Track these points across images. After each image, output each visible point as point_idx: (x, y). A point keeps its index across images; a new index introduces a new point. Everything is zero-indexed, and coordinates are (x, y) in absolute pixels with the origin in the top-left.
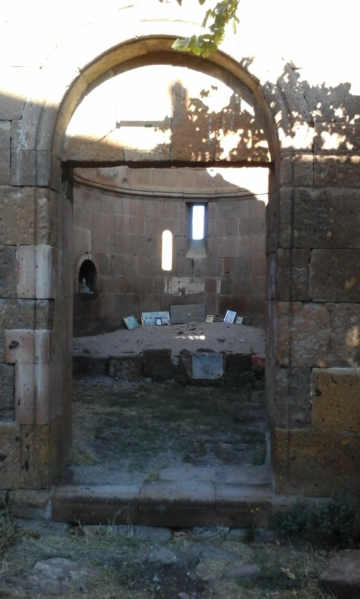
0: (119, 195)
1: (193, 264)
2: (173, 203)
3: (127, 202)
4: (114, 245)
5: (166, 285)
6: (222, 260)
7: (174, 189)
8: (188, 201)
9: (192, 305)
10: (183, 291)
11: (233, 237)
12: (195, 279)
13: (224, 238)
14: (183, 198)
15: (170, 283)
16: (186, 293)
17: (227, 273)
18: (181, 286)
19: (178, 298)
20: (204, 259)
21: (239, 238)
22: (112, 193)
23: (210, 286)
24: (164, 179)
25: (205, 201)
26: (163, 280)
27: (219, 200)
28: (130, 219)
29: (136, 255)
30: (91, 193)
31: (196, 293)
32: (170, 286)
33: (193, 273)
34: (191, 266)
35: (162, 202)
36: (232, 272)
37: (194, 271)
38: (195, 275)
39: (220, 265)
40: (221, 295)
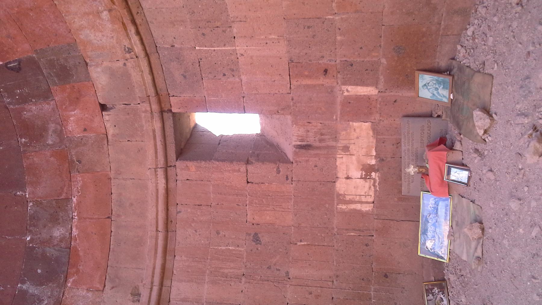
1: (307, 147)
5: (353, 206)
8: (172, 154)
9: (403, 148)
10: (368, 170)
11: (241, 59)
12: (341, 143)
13: (244, 78)
14: (167, 167)
15: (348, 198)
16: (373, 162)
17: (326, 71)
18: (356, 173)
19: (384, 180)
20: (295, 122)
21: (240, 47)
23: (358, 109)
24: (131, 204)
25: (169, 123)
26: (343, 213)
27: (163, 93)
29: (287, 273)
31: (373, 141)
32: (358, 198)
33: (328, 147)
34: (312, 152)
35: (179, 207)
36: (325, 61)
37: (323, 144)
38: (333, 143)
39: (307, 86)
40: (381, 86)
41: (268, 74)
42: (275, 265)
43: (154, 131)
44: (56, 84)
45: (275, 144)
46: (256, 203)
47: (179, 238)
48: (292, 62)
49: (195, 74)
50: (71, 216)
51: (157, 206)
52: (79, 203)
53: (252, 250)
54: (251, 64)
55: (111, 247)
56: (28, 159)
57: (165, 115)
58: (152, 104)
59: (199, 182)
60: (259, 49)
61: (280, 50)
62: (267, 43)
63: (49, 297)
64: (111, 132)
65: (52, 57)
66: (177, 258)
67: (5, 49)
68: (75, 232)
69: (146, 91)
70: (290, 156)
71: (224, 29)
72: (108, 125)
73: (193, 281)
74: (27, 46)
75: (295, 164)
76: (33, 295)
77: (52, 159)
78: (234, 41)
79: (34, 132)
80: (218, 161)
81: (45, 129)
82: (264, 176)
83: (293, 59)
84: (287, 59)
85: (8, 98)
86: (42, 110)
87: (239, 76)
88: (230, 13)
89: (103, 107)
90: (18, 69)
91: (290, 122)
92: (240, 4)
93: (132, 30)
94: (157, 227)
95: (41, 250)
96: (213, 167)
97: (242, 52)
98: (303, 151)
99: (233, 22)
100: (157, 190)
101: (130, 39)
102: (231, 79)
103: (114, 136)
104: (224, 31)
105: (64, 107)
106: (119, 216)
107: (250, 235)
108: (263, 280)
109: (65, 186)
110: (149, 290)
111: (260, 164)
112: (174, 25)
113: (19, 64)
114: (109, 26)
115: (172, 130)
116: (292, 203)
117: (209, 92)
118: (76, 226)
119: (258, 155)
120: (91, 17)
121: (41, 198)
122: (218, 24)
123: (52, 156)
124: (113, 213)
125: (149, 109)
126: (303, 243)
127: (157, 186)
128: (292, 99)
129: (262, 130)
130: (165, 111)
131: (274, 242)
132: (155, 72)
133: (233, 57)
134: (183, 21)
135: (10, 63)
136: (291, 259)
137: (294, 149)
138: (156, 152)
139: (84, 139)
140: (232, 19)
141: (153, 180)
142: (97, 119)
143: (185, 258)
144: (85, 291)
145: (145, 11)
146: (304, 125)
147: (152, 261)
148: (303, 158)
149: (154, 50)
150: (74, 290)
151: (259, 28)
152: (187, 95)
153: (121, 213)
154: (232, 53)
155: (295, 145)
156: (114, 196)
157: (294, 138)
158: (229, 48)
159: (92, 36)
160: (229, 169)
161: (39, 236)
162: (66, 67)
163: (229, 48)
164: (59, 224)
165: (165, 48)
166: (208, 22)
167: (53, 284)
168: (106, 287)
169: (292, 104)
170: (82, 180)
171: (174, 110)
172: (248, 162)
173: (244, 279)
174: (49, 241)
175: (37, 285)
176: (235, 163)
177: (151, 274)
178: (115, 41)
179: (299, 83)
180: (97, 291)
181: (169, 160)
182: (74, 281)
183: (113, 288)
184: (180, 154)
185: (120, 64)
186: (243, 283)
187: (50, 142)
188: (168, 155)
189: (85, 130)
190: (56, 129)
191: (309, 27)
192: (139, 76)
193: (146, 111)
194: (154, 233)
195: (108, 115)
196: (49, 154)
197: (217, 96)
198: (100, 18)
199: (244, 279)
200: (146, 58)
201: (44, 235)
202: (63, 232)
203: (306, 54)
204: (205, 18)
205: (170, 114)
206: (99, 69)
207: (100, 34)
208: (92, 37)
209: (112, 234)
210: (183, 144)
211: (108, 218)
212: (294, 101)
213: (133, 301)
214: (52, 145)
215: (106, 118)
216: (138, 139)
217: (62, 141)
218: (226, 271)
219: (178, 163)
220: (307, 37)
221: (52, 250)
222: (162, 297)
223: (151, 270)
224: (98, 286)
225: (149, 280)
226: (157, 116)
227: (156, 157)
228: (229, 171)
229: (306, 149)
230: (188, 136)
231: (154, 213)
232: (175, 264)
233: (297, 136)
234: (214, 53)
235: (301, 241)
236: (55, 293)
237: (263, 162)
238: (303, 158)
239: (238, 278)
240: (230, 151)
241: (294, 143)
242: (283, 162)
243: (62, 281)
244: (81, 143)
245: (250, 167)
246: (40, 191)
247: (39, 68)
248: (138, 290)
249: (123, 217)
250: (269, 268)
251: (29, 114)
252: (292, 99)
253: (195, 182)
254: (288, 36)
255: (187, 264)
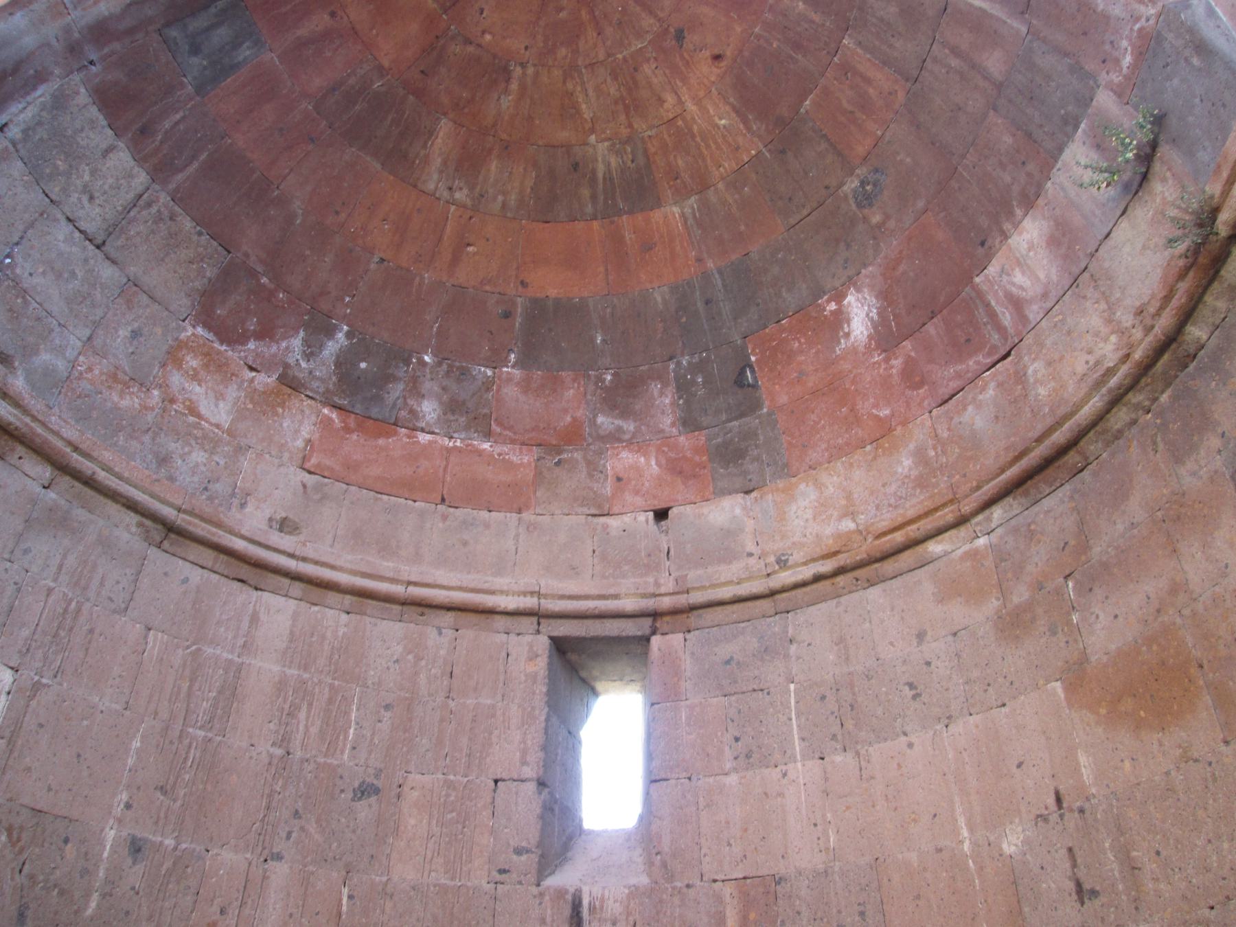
0: (244, 571)
2: (495, 637)
3: (278, 611)
4: (162, 789)
6: (728, 890)
7: (501, 582)
8: (564, 629)
11: (775, 774)
13: (733, 779)
14: (538, 615)
20: (634, 892)
21: (803, 771)
22: (208, 556)
24: (465, 544)
27: (693, 619)
28: (281, 685)
29: (279, 857)
30: (80, 513)
35: (450, 633)
41: (746, 830)
42: (302, 829)
43: (616, 597)
44: (709, 439)
45: (569, 854)
46: (448, 795)
47: (385, 626)
48: (778, 883)
49: (736, 682)
50: (456, 435)
51: (460, 589)
52: (480, 453)
53: (341, 777)
54: (766, 794)
55: (385, 497)
56: (574, 380)
57: (648, 622)
58: (675, 598)
59: (502, 678)
60: (800, 810)
61: (802, 856)
62: (815, 825)
63: (311, 373)
64: (613, 522)
65: (761, 438)
66: (344, 616)
67: (779, 367)
68: (424, 438)
69: (698, 589)
70: (552, 881)
71: (839, 737)
72: (627, 519)
73: (291, 641)
74: (783, 399)
75: (535, 890)
76: (321, 346)
77: (569, 419)
78: (813, 758)
79: (623, 395)
80: (547, 720)
81: (625, 413)
82: (509, 819)
83: (783, 884)
84: (783, 871)
85: (689, 363)
86: (663, 413)
87: (735, 770)
88: (876, 746)
89: (661, 515)
90: (740, 382)
91: (633, 881)
92: (899, 765)
93: (826, 567)
94: (416, 584)
95: (401, 374)
96: (533, 708)
97: (792, 775)
98: (567, 911)
99: (858, 754)
100: (492, 592)
101: (805, 564)
102: (728, 754)
103: (605, 527)
104: (834, 737)
105: (666, 449)
106: (444, 518)
107: (377, 776)
108: (270, 796)
109: (515, 433)
110: (290, 550)
111: (538, 811)
112: (837, 644)
113: (749, 385)
114: (828, 530)
115: (615, 633)
116: (443, 881)
117: (698, 709)
118: (436, 442)
119: (552, 810)
120: (844, 502)
121: (498, 390)
122: (849, 725)
123: (574, 419)
124: (452, 510)
125: (663, 590)
126: (345, 900)
127: (502, 592)
128: (688, 886)
129: (590, 832)
130: (654, 620)
131: (354, 831)
132: (736, 607)
133: (777, 756)
134: (847, 659)
135: (753, 372)
136: (311, 868)
137: (572, 890)
138: (571, 597)
139: (602, 476)
140: (863, 752)
141: (515, 588)
142: (639, 501)
143: (340, 634)
144: (307, 436)
145: (861, 593)
146: (629, 914)
147: (349, 566)
148: (549, 911)
149: (782, 607)
150: (313, 418)
151: (848, 808)
152: (688, 664)
153: (448, 523)
154: (788, 755)
155: (580, 891)
156: (484, 514)
157: (597, 891)
158: (798, 749)
159: (806, 503)
160: (529, 742)
161: (428, 376)
162: (744, 458)
163: (798, 749)
164: (445, 414)
165: (786, 627)
166: (852, 706)
167: (334, 384)
168: (307, 475)
169: (678, 884)
170: (522, 465)
171: (656, 641)
172: (541, 784)
173: (279, 752)
174: (414, 389)
175: (338, 357)
176: (541, 755)
177: (324, 559)
178: (795, 539)
179: (728, 899)
180: (304, 458)
181: (552, 621)
182: (331, 419)
183: (304, 486)
184: (561, 646)
185: (751, 547)
186: (272, 750)
187: (600, 419)
188: (563, 621)
189: (619, 479)
190: (624, 432)
191: (862, 914)
192: (729, 578)
193: (657, 584)
194: (405, 577)
195: (647, 521)
196: (579, 413)
197: (688, 725)
198: (844, 515)
199: (279, 752)
200: (767, 592)
201: (427, 386)
202: (428, 418)
203: (799, 913)
204: (860, 699)
205: (647, 631)
206: (738, 511)
207: (809, 514)
208: (802, 503)
209: (410, 502)
210: (573, 657)
211: (443, 500)
212: (685, 890)
213: (270, 520)
214: (595, 421)
215: (642, 517)
216: (598, 568)
217: (602, 439)
218: (302, 715)
219: (543, 642)
220: (839, 912)
221: (397, 394)
222: (270, 575)
223: (331, 560)
224: (314, 461)
225: (311, 554)
226: (649, 604)
227: (562, 597)
228: (525, 743)
229: (572, 917)
230: (584, 674)
231: (448, 582)
232: (330, 613)
233: (603, 895)
234: (783, 719)
235: (350, 897)
236: (315, 384)
237: (541, 817)
238: (549, 911)
239: (284, 741)
240: (560, 751)
241: (586, 889)
242: (539, 863)
243: (336, 399)
244: (595, 470)
245: (531, 787)
246: (511, 392)
247: (742, 415)
248: (290, 533)
249: (441, 525)
250: (296, 814)
251: (656, 393)
252: (688, 886)
253: (502, 668)
254: (836, 869)
255: (329, 634)
